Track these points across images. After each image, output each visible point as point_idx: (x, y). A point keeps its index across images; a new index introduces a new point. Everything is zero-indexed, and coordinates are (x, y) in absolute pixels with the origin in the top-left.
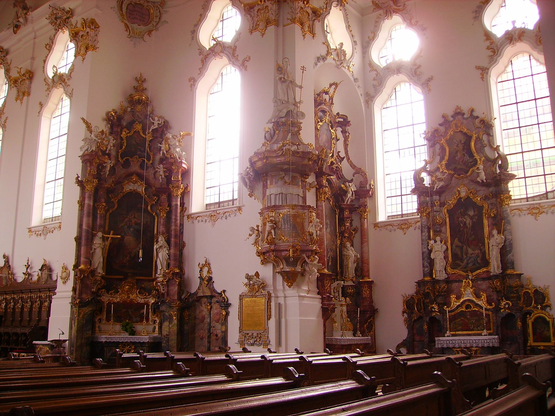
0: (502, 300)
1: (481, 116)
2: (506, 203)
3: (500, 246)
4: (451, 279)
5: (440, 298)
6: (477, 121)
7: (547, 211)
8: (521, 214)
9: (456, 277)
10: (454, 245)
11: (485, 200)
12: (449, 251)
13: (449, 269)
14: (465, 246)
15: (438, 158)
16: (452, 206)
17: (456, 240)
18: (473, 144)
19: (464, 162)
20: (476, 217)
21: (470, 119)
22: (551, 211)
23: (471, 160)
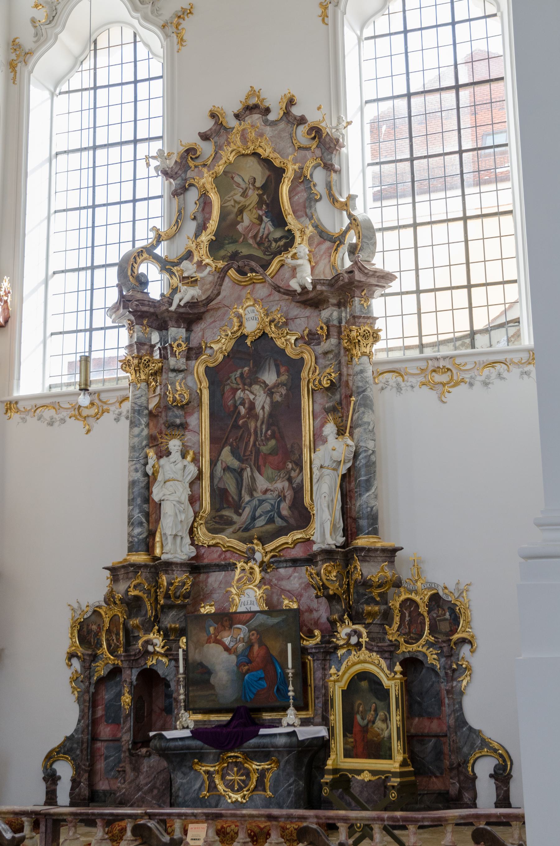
0: (342, 621)
1: (313, 118)
2: (364, 349)
3: (343, 470)
4: (206, 561)
5: (173, 613)
6: (302, 130)
7: (471, 378)
8: (403, 384)
9: (220, 556)
10: (219, 464)
11: (308, 343)
12: (206, 482)
13: (203, 535)
14: (249, 469)
15: (191, 227)
16: (220, 357)
17: (227, 450)
18: (285, 189)
19: (258, 239)
20: (283, 391)
21: (282, 125)
22: (483, 378)
23: (278, 234)
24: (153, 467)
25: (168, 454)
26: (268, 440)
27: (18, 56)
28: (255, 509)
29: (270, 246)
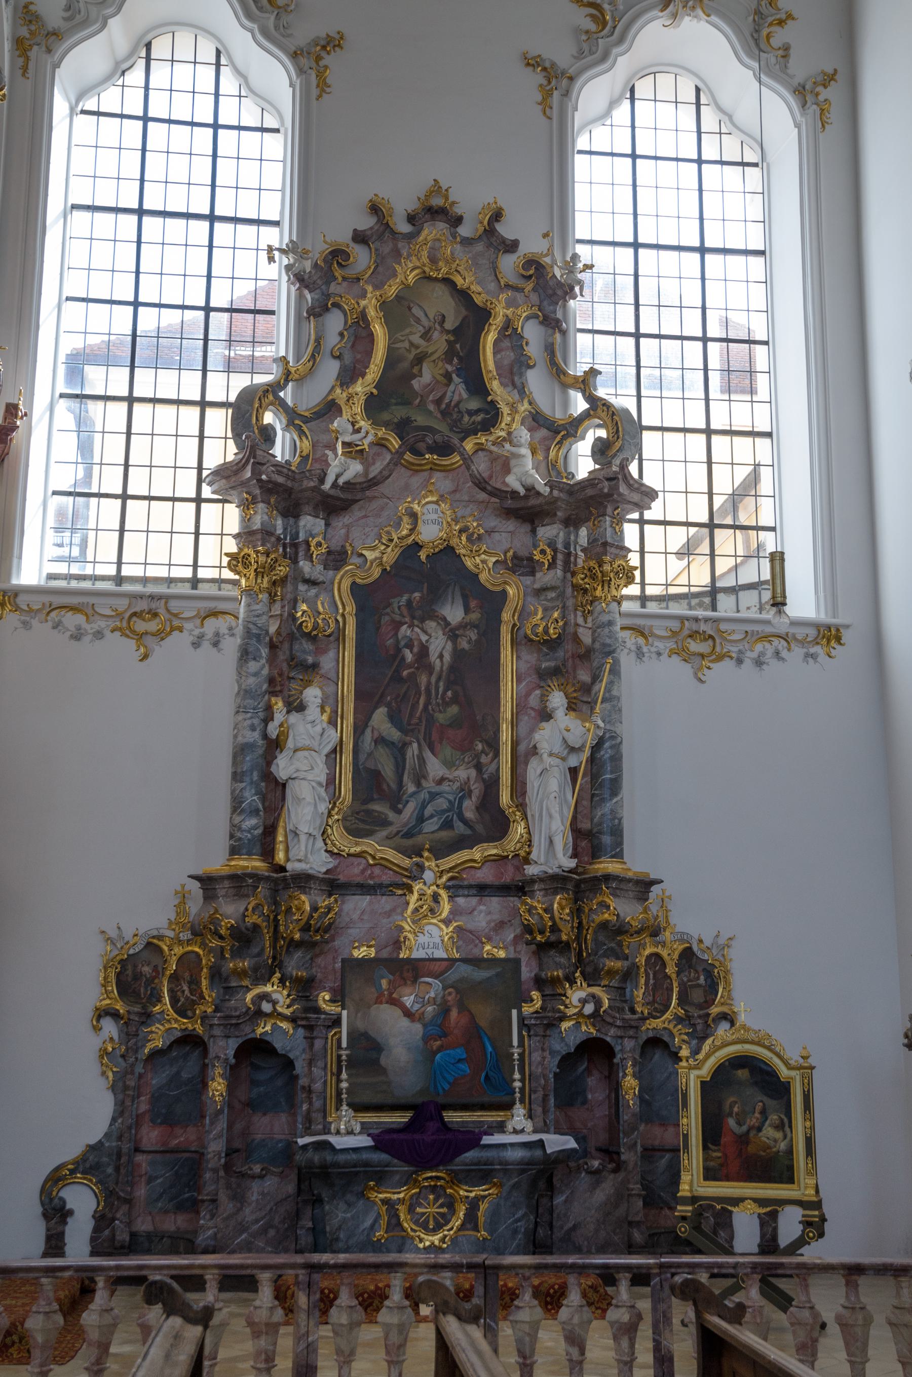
1: (532, 245)
2: (614, 592)
7: (740, 652)
8: (645, 649)
10: (368, 732)
12: (347, 758)
14: (415, 745)
15: (330, 369)
16: (376, 573)
19: (443, 406)
20: (473, 635)
21: (480, 247)
22: (754, 655)
23: (474, 405)
24: (281, 725)
25: (301, 708)
26: (446, 704)
27: (32, 33)
28: (424, 806)
29: (460, 420)
